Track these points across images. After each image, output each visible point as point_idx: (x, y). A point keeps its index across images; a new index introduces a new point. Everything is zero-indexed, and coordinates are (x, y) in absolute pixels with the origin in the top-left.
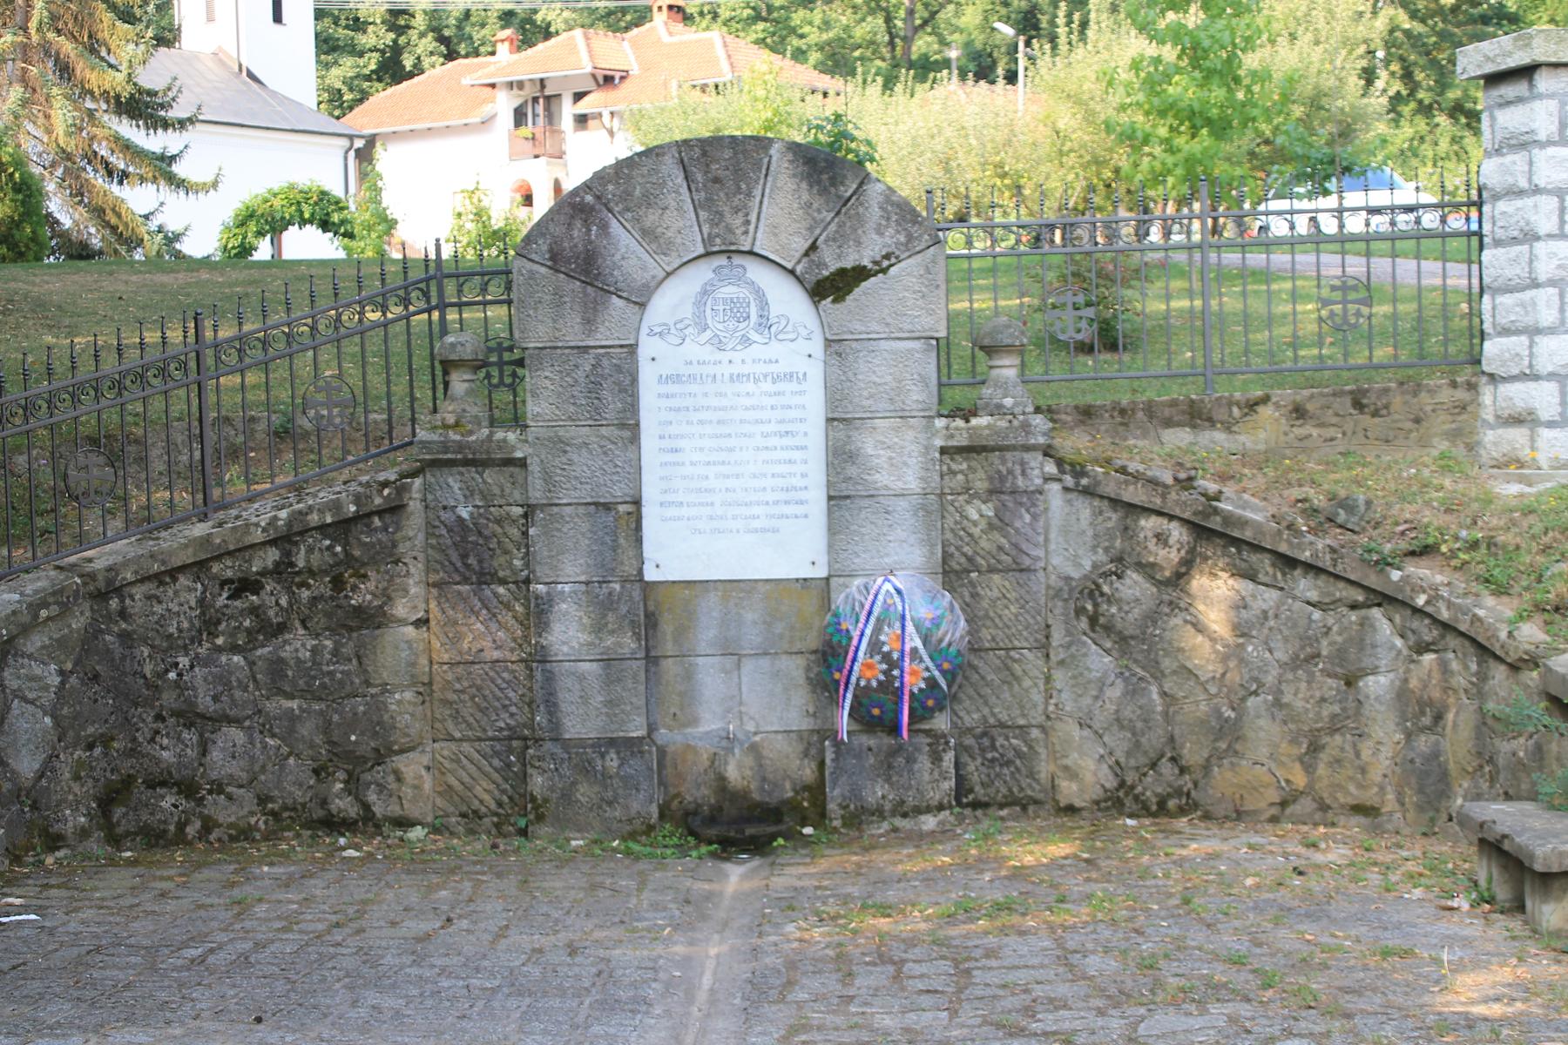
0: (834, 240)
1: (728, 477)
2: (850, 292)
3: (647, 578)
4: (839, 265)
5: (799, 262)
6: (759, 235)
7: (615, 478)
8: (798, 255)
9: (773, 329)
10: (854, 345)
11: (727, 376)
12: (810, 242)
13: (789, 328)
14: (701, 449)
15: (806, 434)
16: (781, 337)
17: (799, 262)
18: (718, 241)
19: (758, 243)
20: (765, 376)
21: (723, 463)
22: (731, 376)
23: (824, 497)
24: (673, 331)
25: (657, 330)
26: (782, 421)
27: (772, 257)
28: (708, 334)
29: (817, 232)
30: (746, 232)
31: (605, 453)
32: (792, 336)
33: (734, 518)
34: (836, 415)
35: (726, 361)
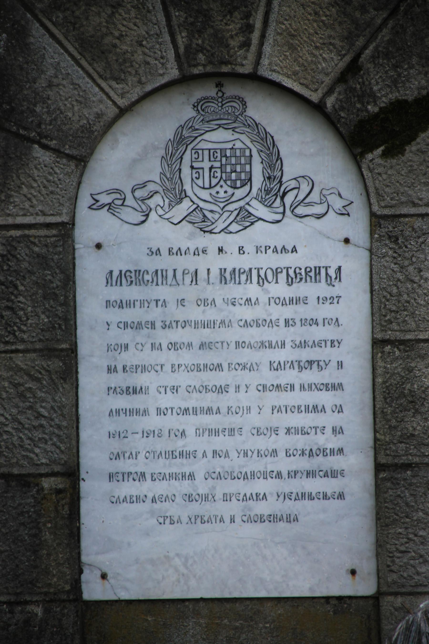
0: (387, 55)
1: (217, 433)
2: (412, 139)
3: (86, 596)
4: (393, 96)
5: (330, 92)
6: (267, 49)
7: (38, 434)
8: (328, 80)
9: (289, 199)
10: (418, 223)
11: (215, 272)
12: (348, 59)
13: (315, 196)
14: (175, 389)
15: (340, 365)
16: (300, 210)
17: (330, 92)
18: (201, 57)
19: (265, 61)
20: (276, 272)
21: (209, 411)
22: (223, 271)
23: (370, 465)
24: (130, 201)
25: (105, 199)
26: (303, 345)
27: (288, 83)
28: (186, 204)
29: (360, 42)
30: (247, 44)
31: (22, 396)
32: (319, 209)
33: (227, 498)
34: (389, 335)
35: (213, 250)
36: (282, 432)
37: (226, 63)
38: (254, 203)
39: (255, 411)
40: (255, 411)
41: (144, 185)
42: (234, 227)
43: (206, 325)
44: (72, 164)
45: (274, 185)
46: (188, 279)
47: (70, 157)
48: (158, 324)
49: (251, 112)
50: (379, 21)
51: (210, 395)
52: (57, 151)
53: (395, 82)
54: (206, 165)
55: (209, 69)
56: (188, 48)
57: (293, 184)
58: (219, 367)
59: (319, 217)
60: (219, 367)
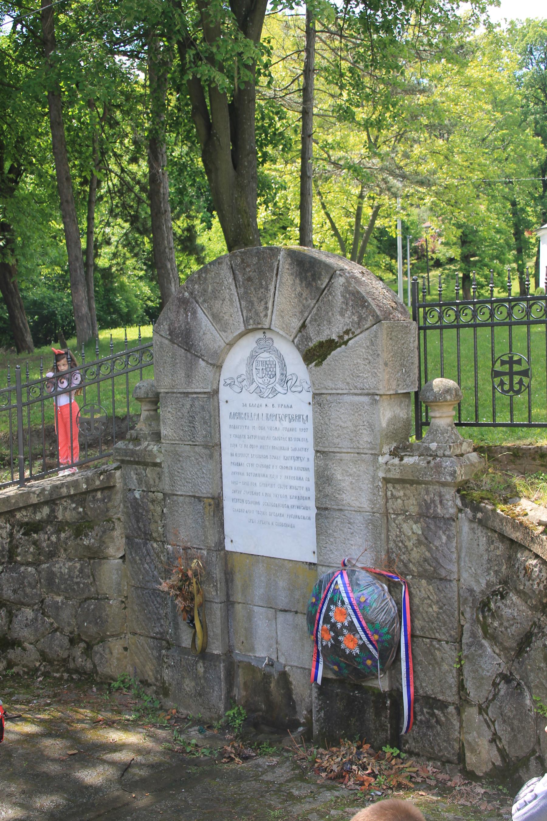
0: (316, 320)
2: (325, 358)
5: (296, 337)
6: (274, 317)
11: (265, 415)
12: (302, 322)
13: (298, 383)
16: (293, 389)
17: (296, 337)
19: (273, 323)
24: (236, 383)
25: (228, 382)
28: (254, 384)
29: (306, 314)
30: (266, 315)
32: (299, 389)
36: (288, 487)
37: (260, 324)
38: (277, 385)
39: (279, 477)
40: (279, 477)
41: (240, 376)
42: (271, 396)
43: (263, 438)
44: (211, 367)
45: (284, 377)
46: (256, 417)
47: (211, 364)
48: (247, 437)
49: (275, 345)
50: (312, 305)
51: (264, 469)
52: (207, 362)
53: (318, 332)
54: (261, 368)
55: (254, 326)
56: (247, 317)
57: (290, 377)
58: (266, 457)
59: (300, 392)
60: (266, 457)
